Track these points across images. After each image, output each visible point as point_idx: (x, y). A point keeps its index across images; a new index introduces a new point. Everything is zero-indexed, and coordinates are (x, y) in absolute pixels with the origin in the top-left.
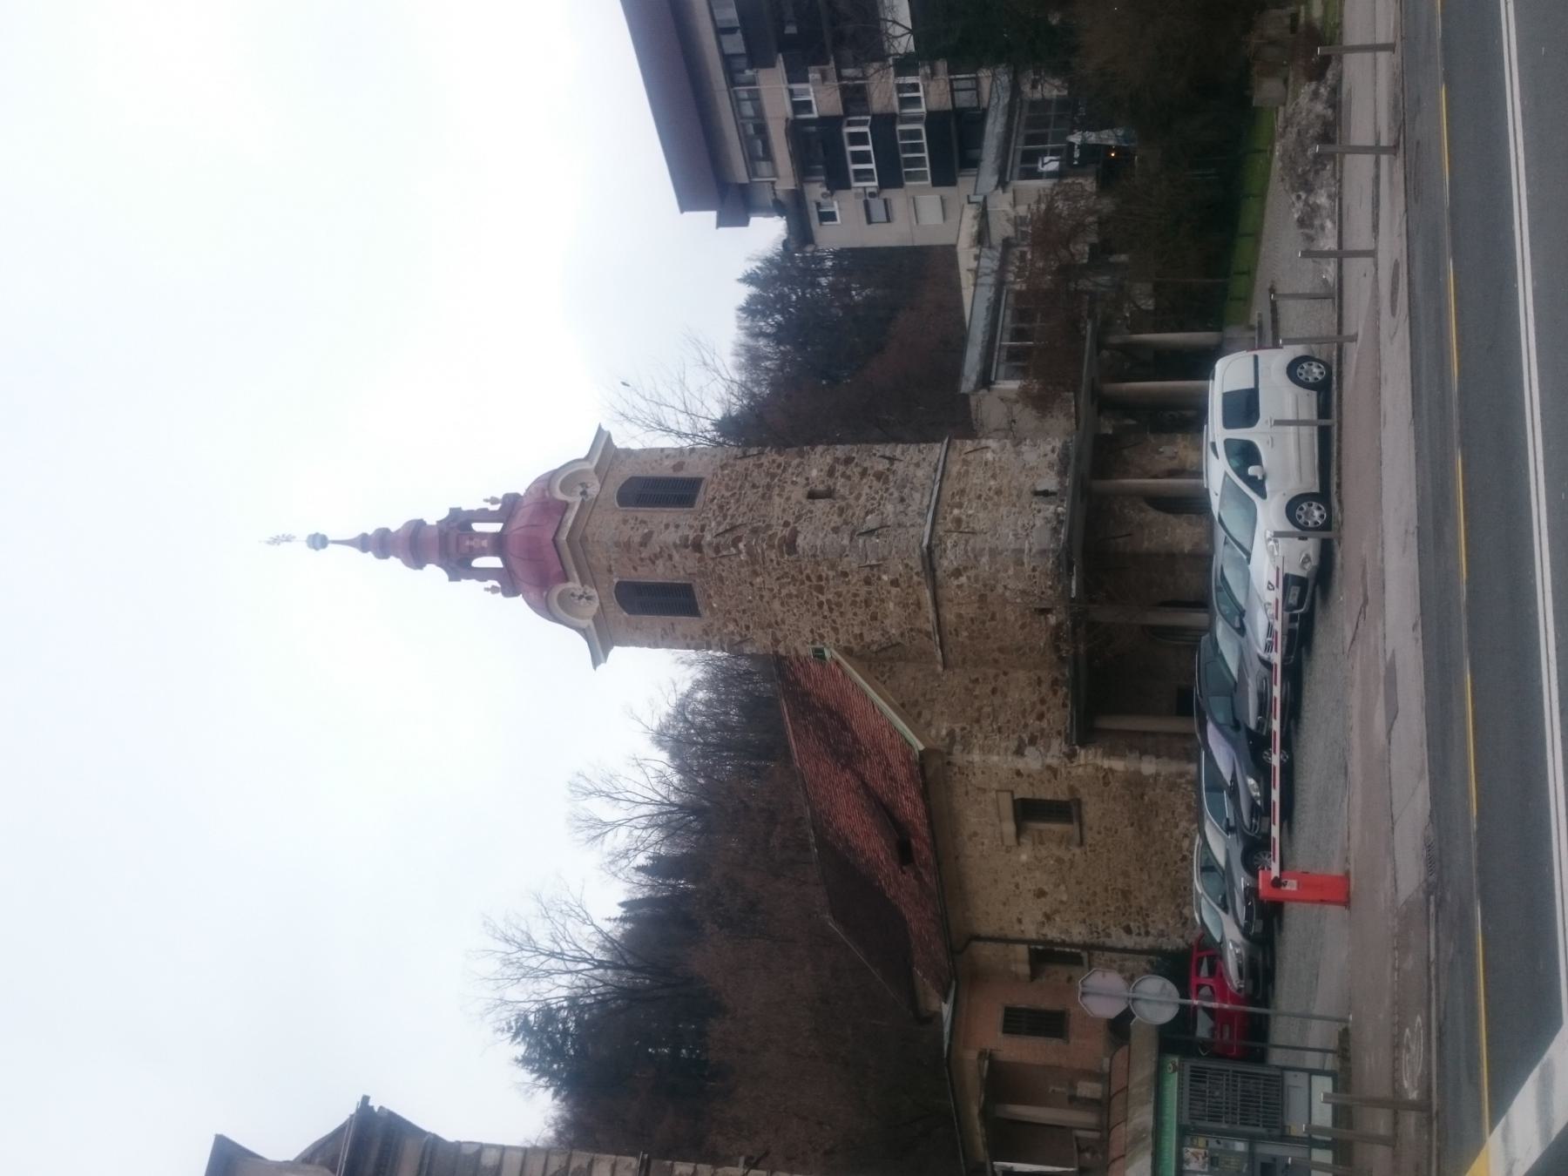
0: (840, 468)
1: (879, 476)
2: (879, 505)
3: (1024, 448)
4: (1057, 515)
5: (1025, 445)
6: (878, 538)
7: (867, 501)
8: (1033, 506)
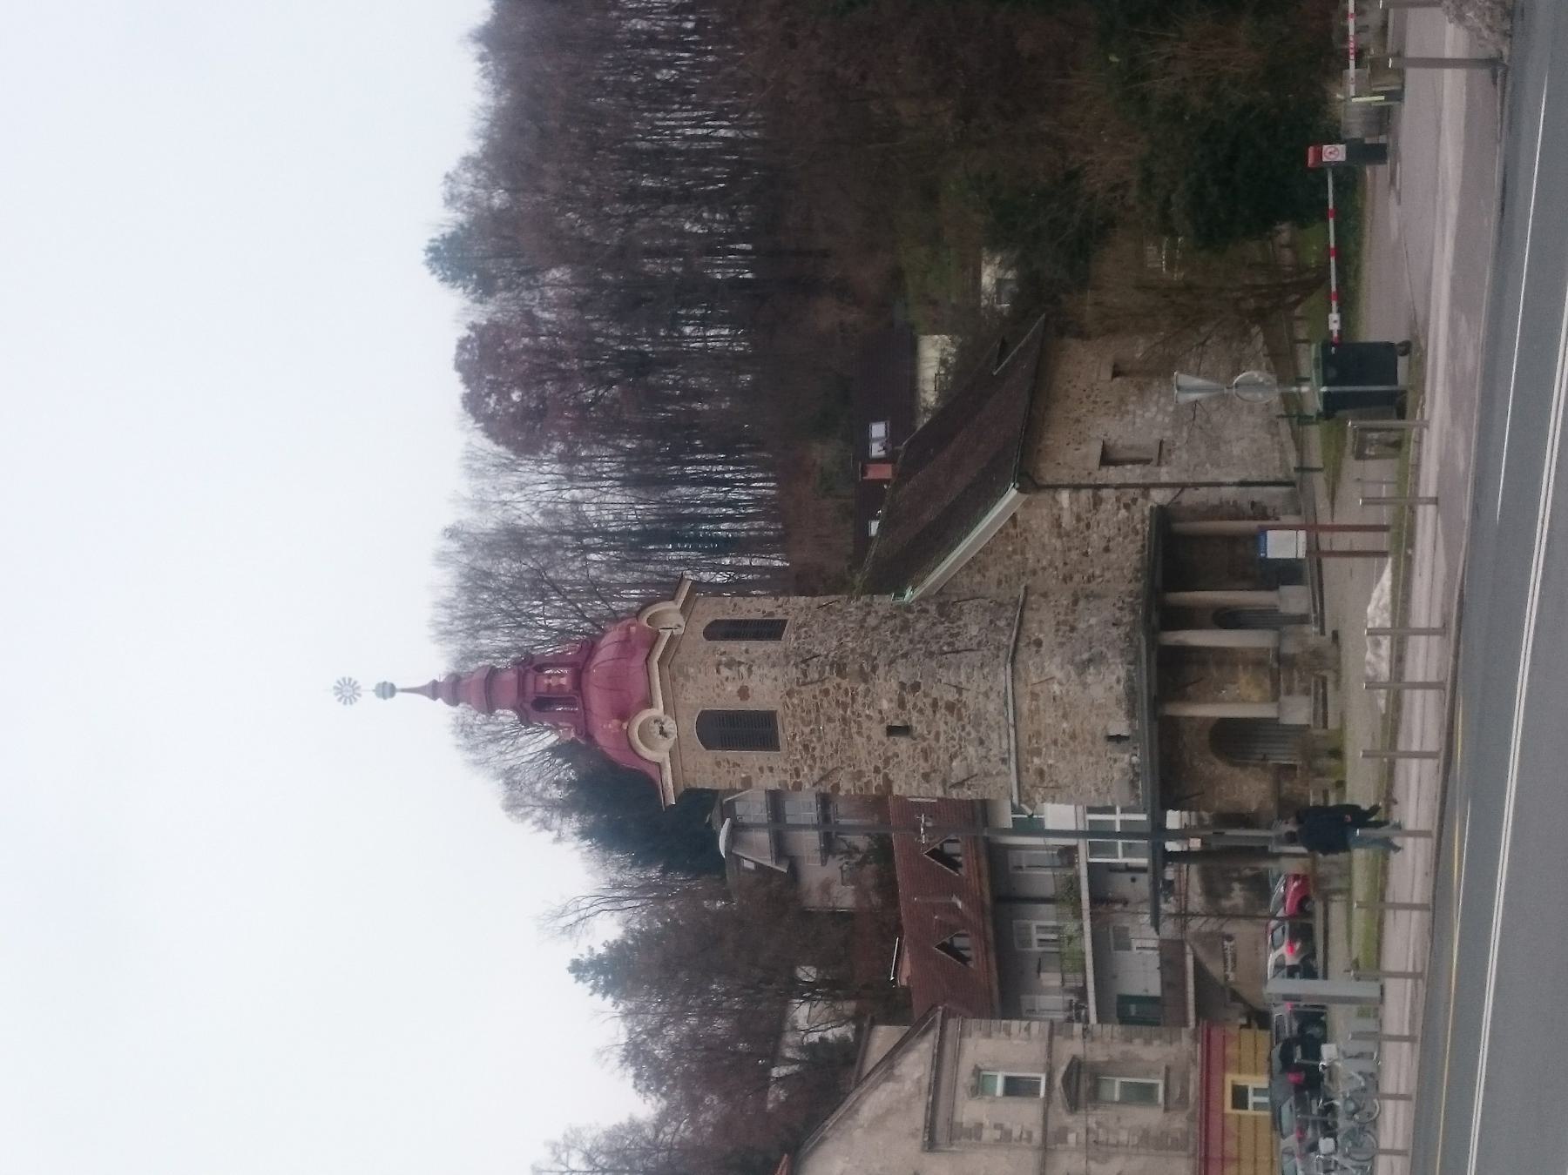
0: (909, 698)
1: (950, 707)
2: (961, 748)
3: (1090, 679)
4: (1132, 766)
6: (969, 789)
7: (947, 741)
8: (1109, 755)
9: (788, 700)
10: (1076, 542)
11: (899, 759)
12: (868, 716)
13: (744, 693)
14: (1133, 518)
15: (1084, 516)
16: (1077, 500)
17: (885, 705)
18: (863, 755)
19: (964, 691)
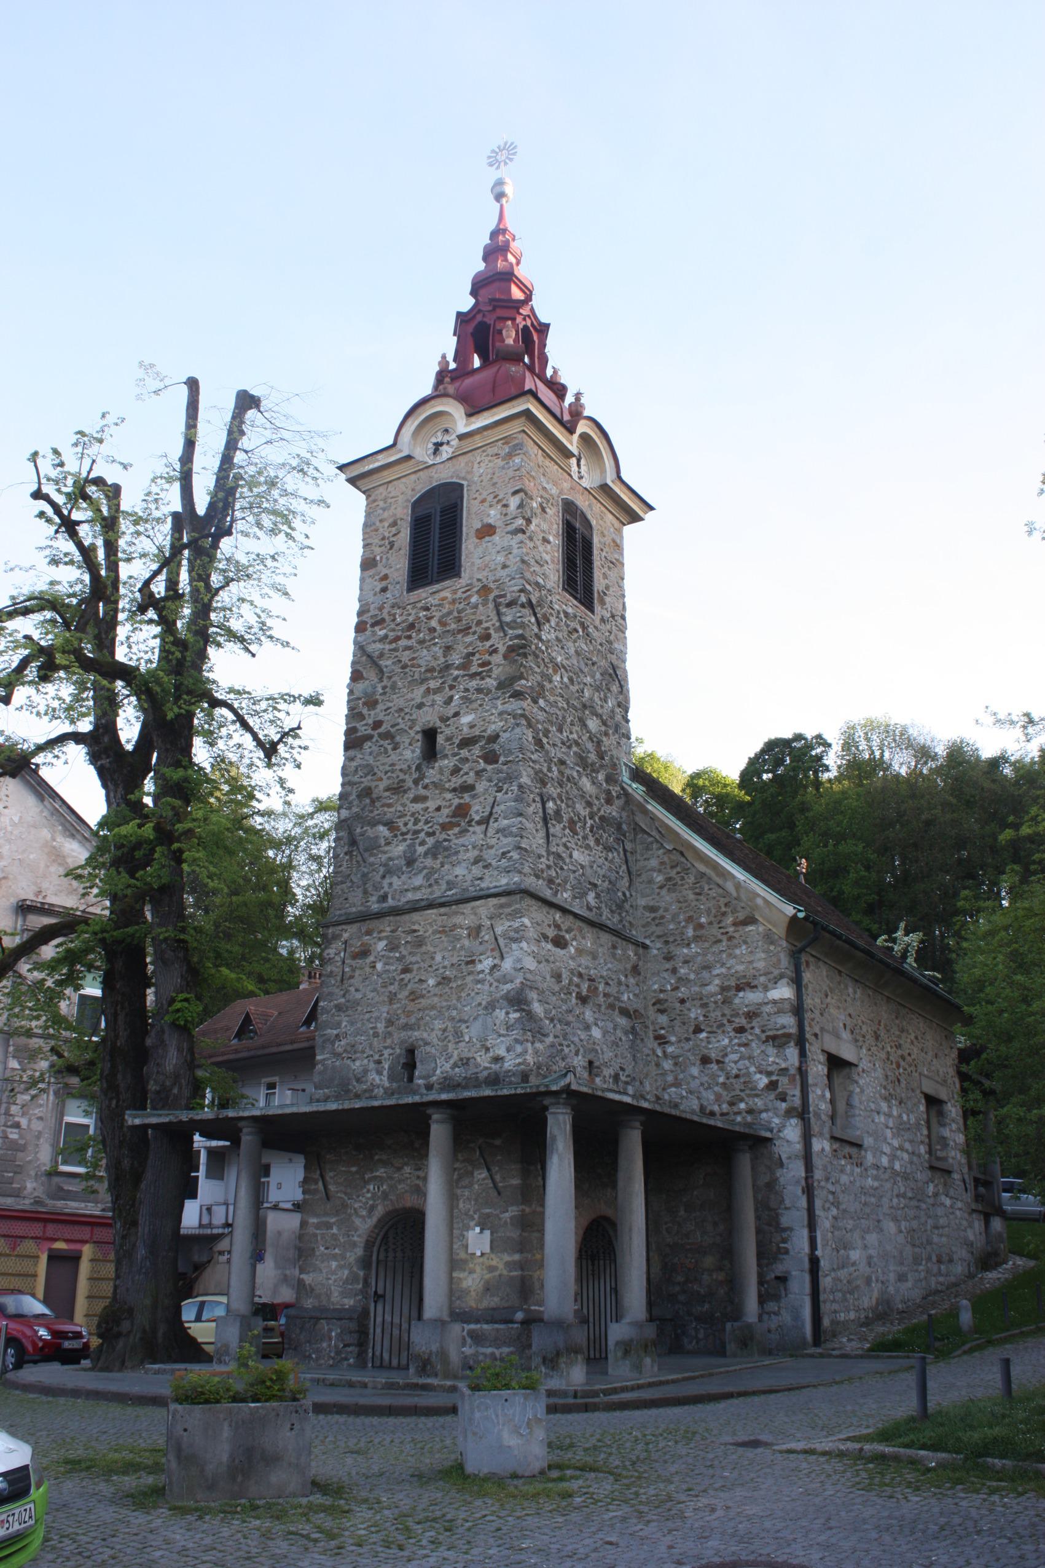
1: (462, 811)
5: (507, 1013)
7: (413, 815)
9: (475, 589)
10: (716, 1014)
11: (390, 752)
12: (451, 698)
13: (487, 531)
14: (757, 1096)
15: (754, 1024)
16: (780, 1011)
17: (466, 719)
18: (398, 702)
19: (484, 827)
